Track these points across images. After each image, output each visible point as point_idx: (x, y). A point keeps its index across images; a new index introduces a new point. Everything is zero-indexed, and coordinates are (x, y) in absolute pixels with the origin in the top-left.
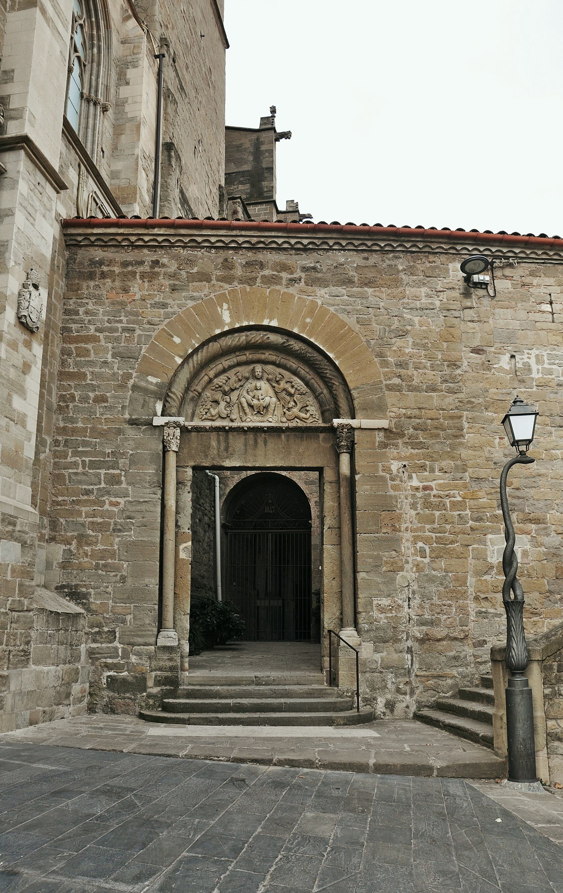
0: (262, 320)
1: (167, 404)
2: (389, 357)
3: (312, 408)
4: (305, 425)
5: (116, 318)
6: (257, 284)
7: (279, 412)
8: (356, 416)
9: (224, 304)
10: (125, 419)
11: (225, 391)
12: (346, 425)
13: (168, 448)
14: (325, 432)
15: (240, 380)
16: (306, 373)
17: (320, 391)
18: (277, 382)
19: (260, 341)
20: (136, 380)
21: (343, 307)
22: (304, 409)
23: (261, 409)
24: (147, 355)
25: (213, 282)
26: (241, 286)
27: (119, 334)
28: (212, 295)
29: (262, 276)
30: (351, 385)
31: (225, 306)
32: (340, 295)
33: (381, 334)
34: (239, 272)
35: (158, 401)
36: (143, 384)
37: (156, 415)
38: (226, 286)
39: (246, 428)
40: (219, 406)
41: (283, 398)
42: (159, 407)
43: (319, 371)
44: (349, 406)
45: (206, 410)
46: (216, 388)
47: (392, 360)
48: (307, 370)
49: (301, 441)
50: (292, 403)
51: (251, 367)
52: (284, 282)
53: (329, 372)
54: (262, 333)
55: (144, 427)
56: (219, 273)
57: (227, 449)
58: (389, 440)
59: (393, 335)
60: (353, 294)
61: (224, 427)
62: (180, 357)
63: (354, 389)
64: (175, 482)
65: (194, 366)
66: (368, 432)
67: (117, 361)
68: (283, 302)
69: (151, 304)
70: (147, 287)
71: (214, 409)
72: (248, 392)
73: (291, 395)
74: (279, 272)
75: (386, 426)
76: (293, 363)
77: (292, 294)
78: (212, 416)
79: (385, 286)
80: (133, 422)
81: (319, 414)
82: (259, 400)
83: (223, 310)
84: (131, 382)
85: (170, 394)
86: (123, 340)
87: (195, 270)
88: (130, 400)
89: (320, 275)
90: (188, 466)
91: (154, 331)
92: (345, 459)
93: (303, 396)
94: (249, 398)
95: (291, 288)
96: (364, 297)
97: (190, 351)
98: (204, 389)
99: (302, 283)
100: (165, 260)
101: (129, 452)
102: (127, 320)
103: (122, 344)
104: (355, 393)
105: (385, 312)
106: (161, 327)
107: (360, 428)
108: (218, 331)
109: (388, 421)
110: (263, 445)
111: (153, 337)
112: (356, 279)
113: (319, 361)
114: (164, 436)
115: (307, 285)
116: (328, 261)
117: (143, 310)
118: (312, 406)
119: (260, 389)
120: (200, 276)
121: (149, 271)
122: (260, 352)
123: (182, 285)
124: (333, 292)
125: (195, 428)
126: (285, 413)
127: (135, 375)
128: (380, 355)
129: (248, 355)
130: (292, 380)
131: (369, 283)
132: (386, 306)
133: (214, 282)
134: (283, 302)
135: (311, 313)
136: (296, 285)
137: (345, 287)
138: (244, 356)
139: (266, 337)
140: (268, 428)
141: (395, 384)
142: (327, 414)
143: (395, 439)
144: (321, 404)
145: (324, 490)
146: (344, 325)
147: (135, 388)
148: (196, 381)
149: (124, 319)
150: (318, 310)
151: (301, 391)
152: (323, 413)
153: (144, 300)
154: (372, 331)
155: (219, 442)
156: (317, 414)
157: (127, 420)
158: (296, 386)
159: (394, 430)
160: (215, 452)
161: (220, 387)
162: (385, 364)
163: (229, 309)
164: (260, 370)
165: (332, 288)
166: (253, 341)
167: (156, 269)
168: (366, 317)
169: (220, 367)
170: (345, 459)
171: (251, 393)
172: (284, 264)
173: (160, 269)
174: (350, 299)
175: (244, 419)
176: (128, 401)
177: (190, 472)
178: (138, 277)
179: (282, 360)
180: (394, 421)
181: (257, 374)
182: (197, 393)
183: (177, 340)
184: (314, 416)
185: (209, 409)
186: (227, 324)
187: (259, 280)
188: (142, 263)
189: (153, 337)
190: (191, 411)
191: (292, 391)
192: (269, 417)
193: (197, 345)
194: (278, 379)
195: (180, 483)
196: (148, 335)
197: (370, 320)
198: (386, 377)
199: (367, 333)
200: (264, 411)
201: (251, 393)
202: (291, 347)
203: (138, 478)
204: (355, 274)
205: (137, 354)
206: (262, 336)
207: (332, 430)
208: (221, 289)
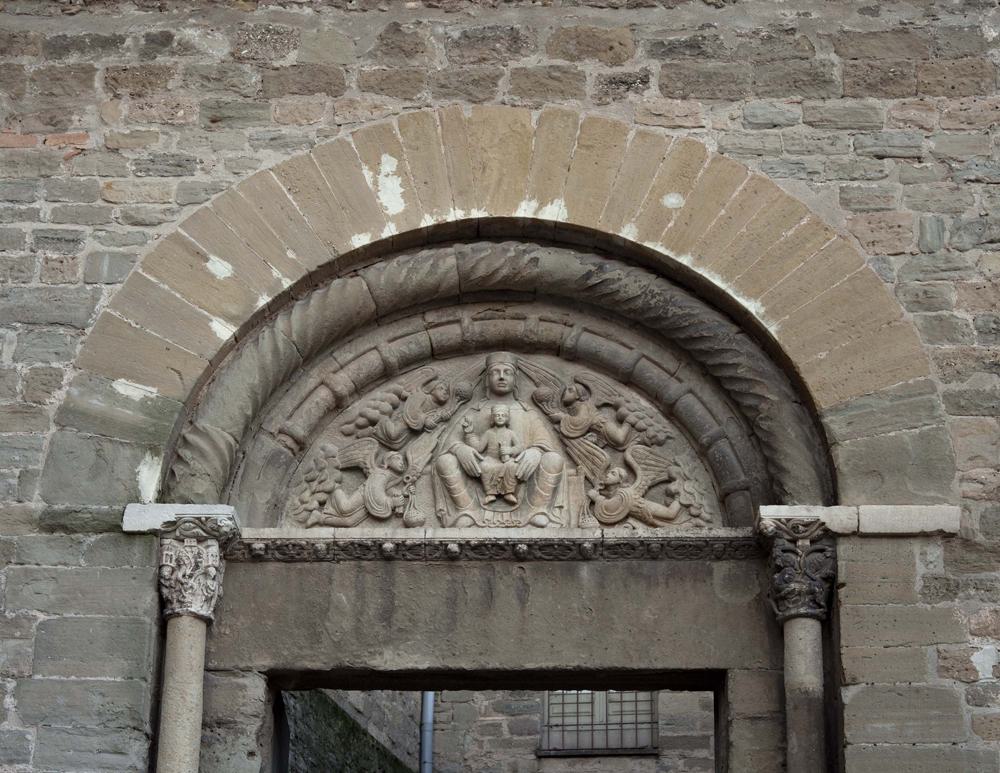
0: (519, 197)
1: (179, 469)
2: (958, 305)
3: (689, 486)
4: (660, 533)
5: (17, 206)
6: (499, 97)
7: (571, 497)
8: (843, 497)
9: (385, 158)
10: (29, 513)
12: (806, 525)
13: (176, 605)
16: (665, 376)
17: (716, 428)
19: (504, 272)
20: (75, 391)
21: (794, 158)
22: (663, 487)
23: (511, 486)
24: (117, 314)
25: (347, 95)
26: (446, 103)
27: (27, 253)
28: (343, 133)
29: (516, 72)
30: (822, 399)
31: (389, 163)
32: (781, 120)
33: (928, 237)
34: (437, 61)
35: (148, 457)
36: (96, 403)
37: (136, 498)
38: (394, 105)
39: (454, 547)
40: (367, 482)
42: (149, 477)
43: (710, 362)
44: (817, 467)
47: (969, 318)
48: (671, 365)
51: (478, 362)
52: (590, 88)
53: (744, 358)
54: (513, 248)
55: (93, 538)
56: (369, 67)
57: (387, 615)
58: (963, 571)
59: (967, 240)
60: (827, 115)
61: (378, 545)
62: (229, 318)
63: (835, 410)
64: (196, 717)
65: (276, 351)
66: (886, 546)
67: (11, 334)
68: (588, 147)
69: (137, 162)
70: (125, 112)
71: (350, 493)
72: (465, 439)
73: (614, 446)
74: (572, 58)
75: (952, 526)
76: (624, 347)
77: (616, 124)
78: (342, 513)
79: (939, 89)
80: (54, 524)
81: (711, 506)
82: (500, 457)
83: (381, 178)
84: (58, 397)
85: (191, 437)
86: (38, 270)
87: (292, 57)
88: (51, 455)
89: (711, 65)
90: (249, 670)
91: (142, 244)
92: (804, 637)
94: (468, 452)
95: (614, 106)
96: (864, 125)
97: (263, 301)
98: (316, 429)
99: (653, 90)
100: (191, 34)
101: (35, 618)
102: (54, 211)
103: (34, 284)
104: (835, 424)
105: (939, 170)
106: (165, 230)
107: (857, 534)
108: (360, 240)
109: (957, 509)
110: (515, 602)
111: (141, 258)
112: (836, 73)
114: (161, 567)
115: (670, 96)
116: (740, 23)
117: (109, 180)
119: (507, 425)
120: (306, 77)
121: (136, 64)
122: (511, 311)
123: (245, 106)
124: (759, 112)
125: (278, 548)
127: (69, 375)
128: (925, 301)
129: (466, 322)
130: (618, 399)
131: (885, 81)
132: (946, 151)
133: (353, 92)
134: (588, 147)
135: (682, 179)
136: (631, 96)
137: (799, 98)
139: (527, 258)
140: (532, 544)
141: (978, 393)
142: (739, 501)
143: (982, 569)
144: (716, 470)
145: (729, 745)
146: (792, 210)
147: (68, 415)
148: (288, 403)
149: (45, 208)
150: (707, 171)
152: (723, 500)
153: (116, 150)
154: (896, 228)
155: (361, 595)
156: (706, 505)
157: (36, 516)
158: (631, 418)
159: (980, 538)
160: (347, 624)
162: (943, 329)
163: (399, 171)
164: (509, 367)
165: (754, 101)
166: (482, 271)
167: (162, 60)
168: (874, 185)
169: (372, 361)
170: (804, 637)
171: (474, 439)
172: (591, 35)
173: (175, 59)
174: (819, 133)
175: (450, 520)
176: (42, 457)
177: (256, 689)
178: (98, 83)
179: (586, 337)
180: (979, 508)
181: (496, 377)
182: (290, 442)
183: (220, 268)
186: (394, 218)
187: (503, 85)
188: (113, 43)
189: (141, 258)
190: (268, 496)
191: (620, 433)
192: (538, 512)
193: (287, 284)
194: (569, 396)
195: (213, 725)
196: (124, 255)
197: (887, 196)
198: (949, 371)
199: (877, 236)
200: (522, 493)
201: (474, 439)
202: (615, 287)
203: (61, 700)
204: (834, 57)
205: (81, 313)
206: (512, 254)
207: (760, 548)
208: (377, 113)
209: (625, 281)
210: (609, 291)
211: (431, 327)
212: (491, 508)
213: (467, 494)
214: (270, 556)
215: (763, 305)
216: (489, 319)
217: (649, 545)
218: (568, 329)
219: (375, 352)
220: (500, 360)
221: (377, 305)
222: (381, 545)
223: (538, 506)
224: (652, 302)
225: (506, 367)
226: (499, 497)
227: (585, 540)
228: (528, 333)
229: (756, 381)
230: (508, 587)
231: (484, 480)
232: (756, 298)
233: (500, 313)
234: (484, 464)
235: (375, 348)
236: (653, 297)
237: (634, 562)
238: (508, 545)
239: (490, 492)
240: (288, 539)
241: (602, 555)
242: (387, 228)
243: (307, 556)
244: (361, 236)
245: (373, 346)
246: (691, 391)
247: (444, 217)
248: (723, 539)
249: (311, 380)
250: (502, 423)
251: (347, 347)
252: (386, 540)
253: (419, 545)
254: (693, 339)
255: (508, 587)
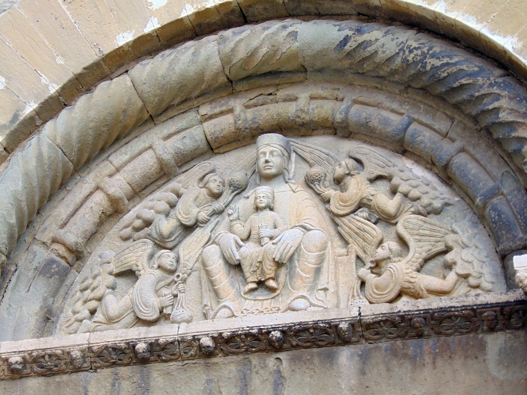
11: (161, 235)
14: (507, 327)
15: (216, 196)
17: (491, 184)
18: (338, 182)
19: (264, 50)
39: (207, 341)
41: (360, 233)
45: (93, 304)
46: (137, 229)
49: (415, 367)
50: (392, 245)
61: (131, 346)
65: (40, 157)
82: (259, 241)
93: (433, 219)
113: (470, 75)
118: (465, 246)
122: (282, 94)
125: (35, 360)
126: (363, 284)
138: (229, 119)
151: (425, 200)
161: (148, 223)
166: (242, 53)
179: (355, 109)
182: (62, 250)
184: (472, 281)
185: (100, 299)
193: (53, 89)
209: (382, 40)
210: (367, 54)
211: (206, 120)
212: (251, 297)
213: (227, 285)
214: (28, 371)
215: (519, 40)
216: (262, 105)
217: (410, 320)
218: (338, 103)
219: (150, 151)
220: (266, 143)
221: (143, 101)
222: (134, 347)
223: (298, 290)
224: (410, 58)
225: (272, 149)
226: (261, 284)
227: (341, 320)
228: (299, 113)
229: (518, 122)
230: (264, 381)
231: (243, 267)
232: (512, 34)
233: (271, 97)
234: (242, 249)
235: (150, 147)
236: (411, 52)
237: (399, 342)
238: (262, 334)
239: (249, 280)
240: (44, 350)
241: (362, 336)
242: (150, 22)
243: (64, 367)
244: (125, 34)
245: (147, 145)
246: (462, 150)
247: (204, 4)
248: (492, 306)
249: (86, 185)
250: (263, 205)
251: (123, 149)
252: (139, 340)
253: (172, 343)
254: (454, 90)
255: (264, 381)
